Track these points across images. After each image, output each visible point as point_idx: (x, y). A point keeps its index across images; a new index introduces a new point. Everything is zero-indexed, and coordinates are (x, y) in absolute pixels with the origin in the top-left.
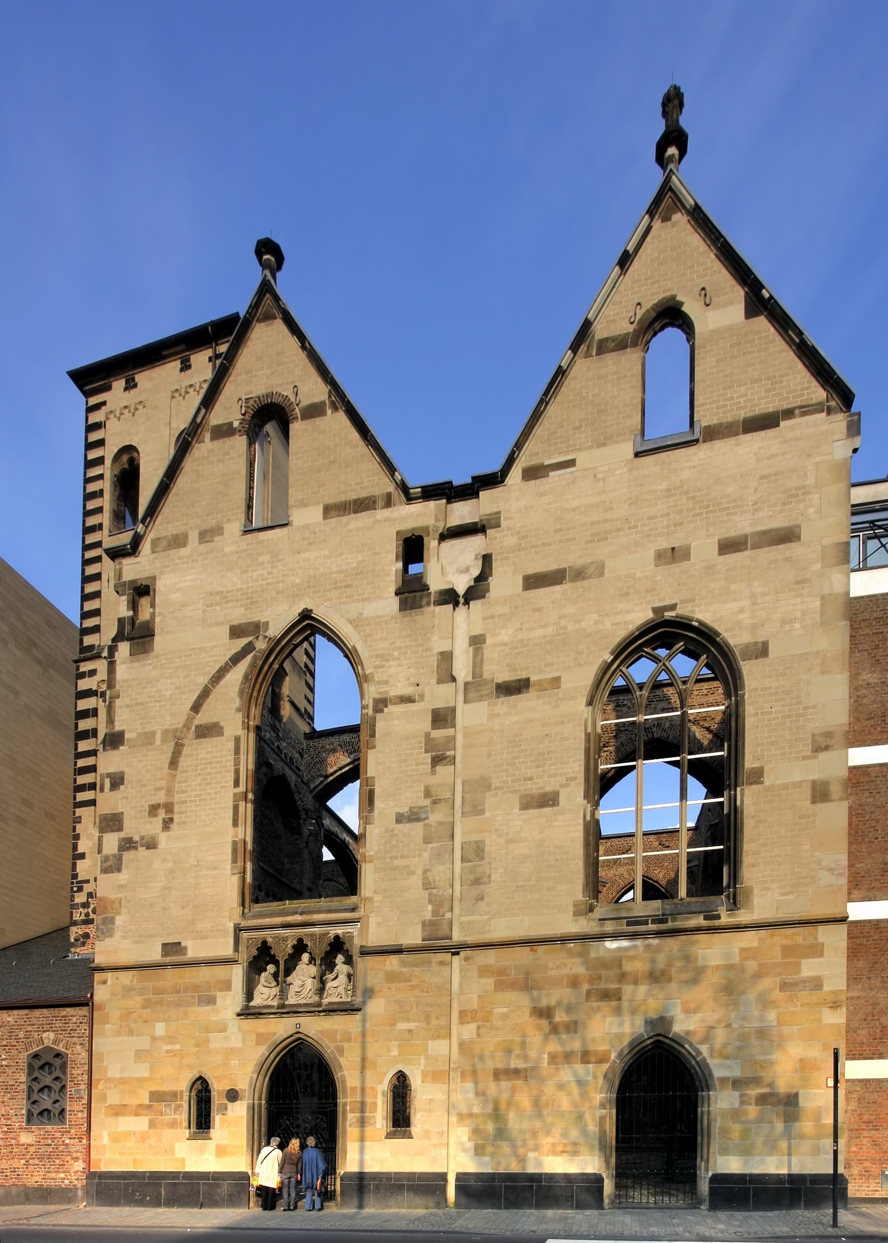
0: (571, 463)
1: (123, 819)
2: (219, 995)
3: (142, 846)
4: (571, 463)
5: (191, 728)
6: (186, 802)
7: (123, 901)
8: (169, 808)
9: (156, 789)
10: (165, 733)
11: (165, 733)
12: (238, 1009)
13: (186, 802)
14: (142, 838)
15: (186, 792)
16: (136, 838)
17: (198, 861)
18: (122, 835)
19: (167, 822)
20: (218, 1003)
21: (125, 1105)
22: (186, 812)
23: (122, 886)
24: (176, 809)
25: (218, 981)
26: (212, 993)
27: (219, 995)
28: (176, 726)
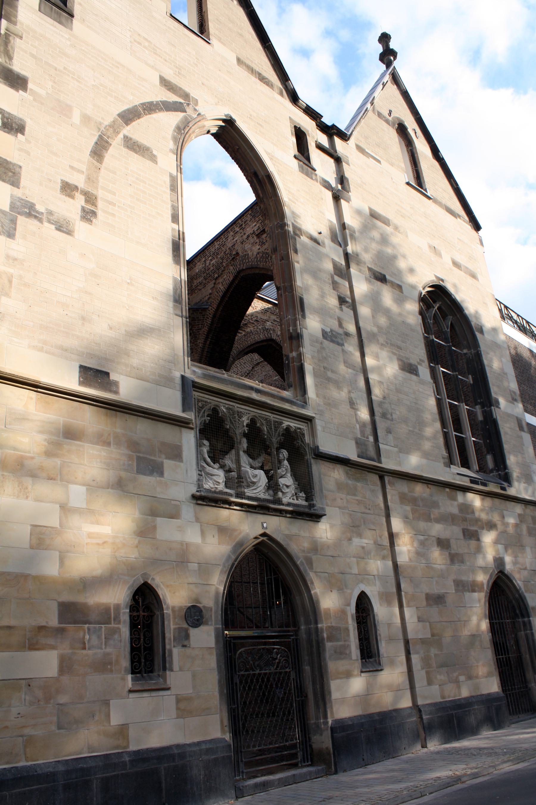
0: (379, 162)
1: (20, 174)
2: (168, 464)
3: (49, 221)
4: (379, 162)
5: (118, 133)
6: (114, 205)
7: (14, 280)
8: (90, 198)
9: (72, 167)
10: (86, 119)
11: (86, 119)
12: (193, 490)
13: (114, 205)
14: (50, 213)
15: (114, 194)
16: (40, 208)
17: (131, 279)
18: (18, 193)
19: (88, 212)
20: (166, 474)
21: (9, 627)
22: (113, 215)
23: (15, 259)
24: (100, 204)
25: (163, 444)
26: (159, 460)
27: (168, 464)
28: (100, 120)
